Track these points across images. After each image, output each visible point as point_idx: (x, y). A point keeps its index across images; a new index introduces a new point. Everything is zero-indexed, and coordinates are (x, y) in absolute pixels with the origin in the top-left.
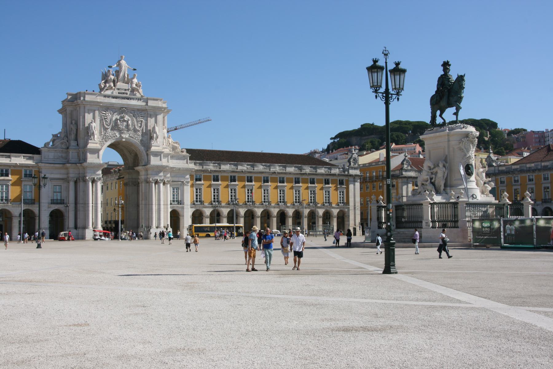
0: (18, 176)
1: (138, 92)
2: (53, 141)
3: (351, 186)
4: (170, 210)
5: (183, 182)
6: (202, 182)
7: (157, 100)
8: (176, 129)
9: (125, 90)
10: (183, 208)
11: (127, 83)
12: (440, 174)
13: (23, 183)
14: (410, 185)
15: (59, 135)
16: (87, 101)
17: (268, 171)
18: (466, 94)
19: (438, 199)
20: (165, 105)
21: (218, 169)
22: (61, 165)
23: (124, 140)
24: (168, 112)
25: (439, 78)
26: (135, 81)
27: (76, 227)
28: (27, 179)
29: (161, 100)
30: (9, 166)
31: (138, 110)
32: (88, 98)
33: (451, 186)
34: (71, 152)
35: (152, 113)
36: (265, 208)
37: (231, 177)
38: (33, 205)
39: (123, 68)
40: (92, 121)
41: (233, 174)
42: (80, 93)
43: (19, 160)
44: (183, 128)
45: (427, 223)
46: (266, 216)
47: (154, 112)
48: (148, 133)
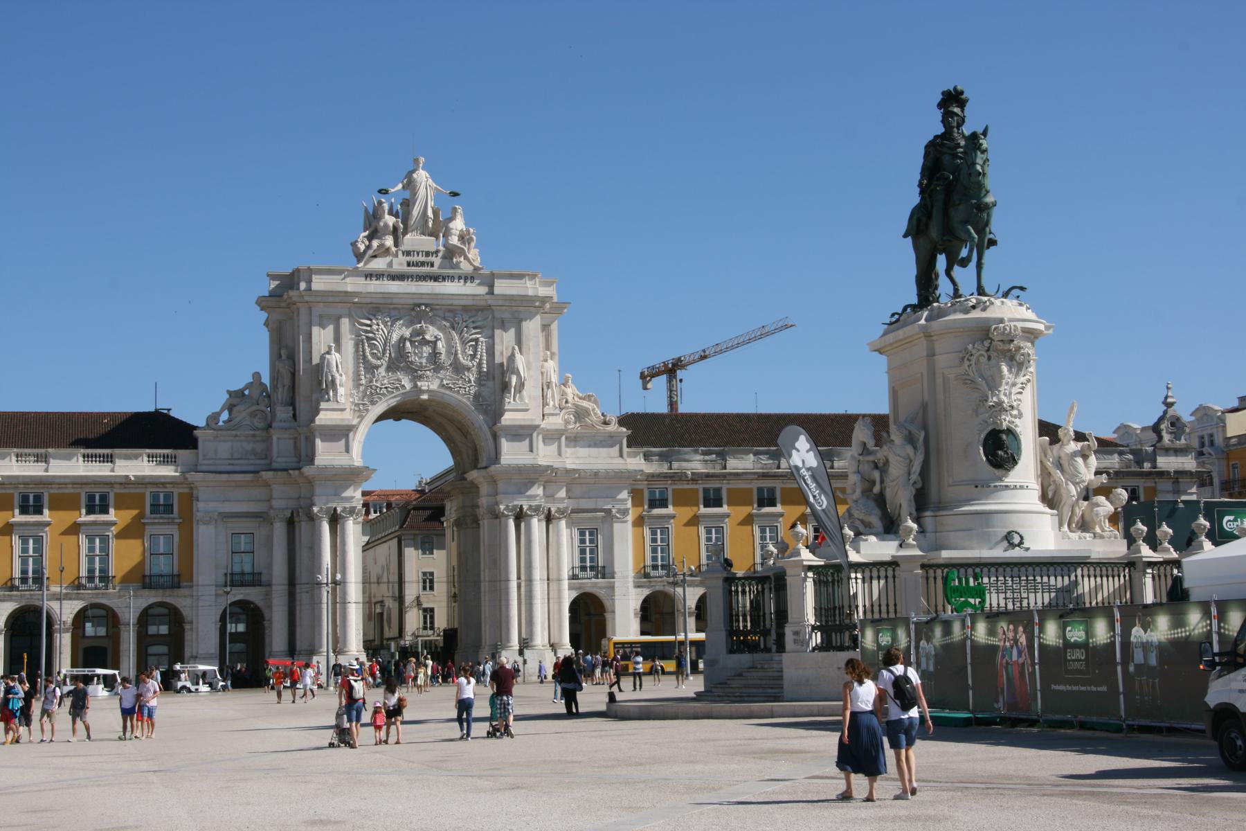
0: (135, 512)
1: (466, 258)
2: (230, 407)
4: (567, 597)
5: (609, 511)
6: (670, 510)
7: (520, 277)
8: (703, 358)
9: (428, 254)
10: (612, 588)
11: (434, 234)
12: (896, 469)
13: (149, 530)
15: (247, 392)
20: (543, 291)
21: (718, 470)
22: (249, 477)
23: (425, 397)
25: (927, 147)
26: (458, 225)
28: (157, 518)
29: (533, 277)
31: (466, 309)
32: (319, 283)
34: (275, 438)
35: (506, 315)
38: (176, 592)
39: (421, 192)
40: (334, 350)
42: (298, 270)
43: (137, 466)
44: (721, 352)
45: (796, 633)
47: (513, 313)
48: (497, 374)
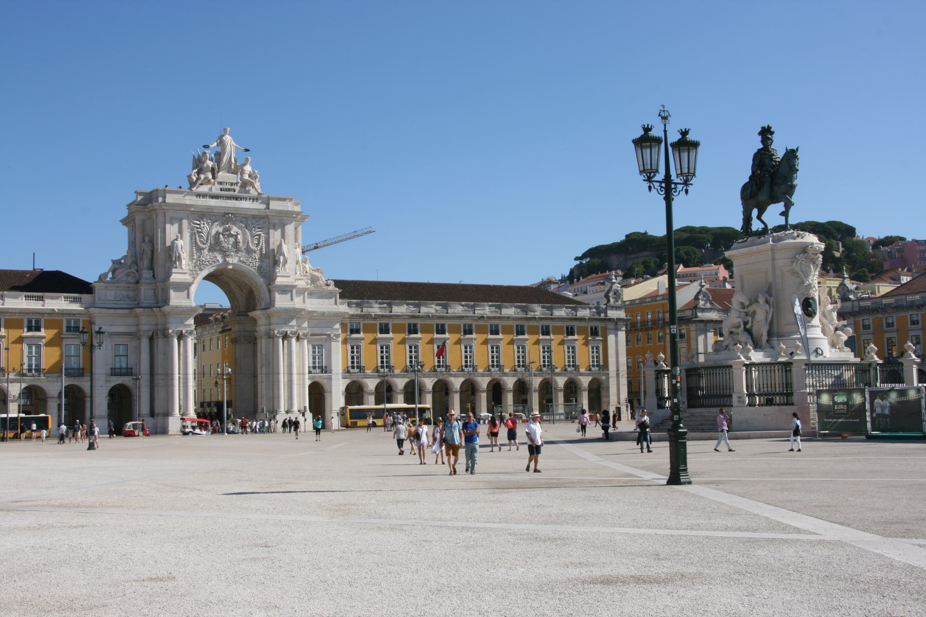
0: (56, 331)
1: (254, 187)
2: (114, 271)
3: (611, 338)
4: (308, 383)
5: (329, 335)
6: (361, 335)
7: (284, 200)
8: (316, 248)
9: (232, 184)
10: (330, 379)
11: (235, 172)
12: (760, 316)
13: (65, 342)
14: (710, 335)
15: (123, 261)
16: (169, 204)
17: (471, 314)
18: (800, 180)
19: (757, 357)
20: (297, 209)
21: (387, 313)
22: (126, 311)
23: (230, 267)
24: (304, 218)
25: (755, 155)
26: (248, 168)
27: (152, 414)
28: (70, 335)
29: (291, 200)
30: (41, 313)
31: (253, 217)
32: (170, 199)
33: (780, 336)
34: (142, 289)
35: (276, 222)
36: (467, 377)
37: (409, 325)
38: (82, 378)
39: (228, 148)
40: (179, 237)
41: (413, 321)
42: (157, 190)
43: (58, 303)
44: (327, 245)
45: (740, 397)
46: (470, 389)
47: (280, 221)
48: (271, 255)
